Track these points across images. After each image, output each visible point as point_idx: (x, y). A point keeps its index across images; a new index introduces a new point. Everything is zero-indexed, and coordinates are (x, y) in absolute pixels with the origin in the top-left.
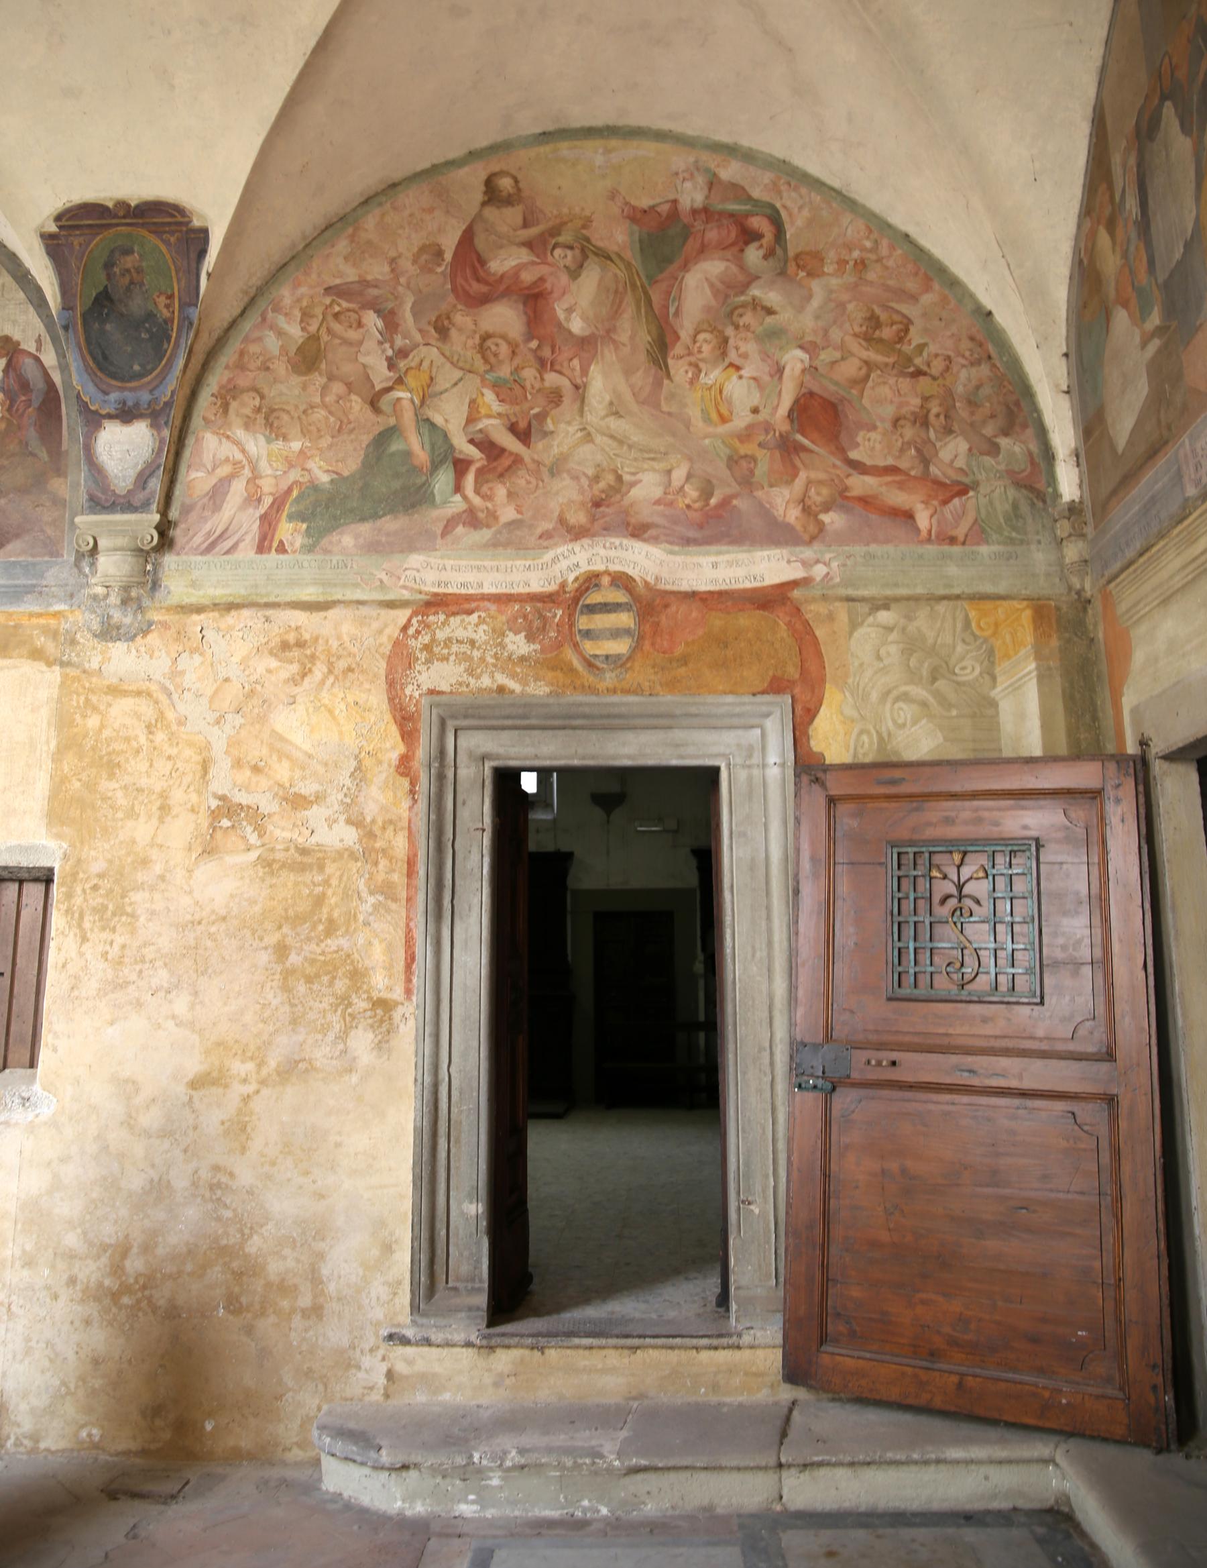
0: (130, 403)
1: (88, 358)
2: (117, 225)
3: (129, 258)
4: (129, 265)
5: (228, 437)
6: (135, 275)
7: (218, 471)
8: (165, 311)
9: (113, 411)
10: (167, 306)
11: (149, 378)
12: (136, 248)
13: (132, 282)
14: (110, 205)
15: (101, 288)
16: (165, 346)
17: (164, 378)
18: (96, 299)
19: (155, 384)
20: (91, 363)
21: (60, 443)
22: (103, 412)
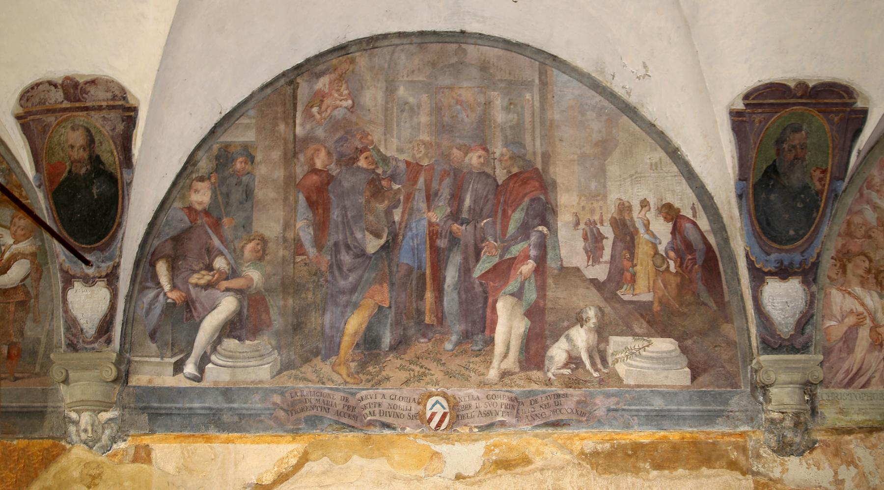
0: (786, 263)
1: (756, 223)
2: (794, 104)
3: (797, 136)
4: (796, 142)
5: (849, 293)
6: (799, 151)
7: (846, 320)
8: (818, 184)
9: (773, 269)
10: (820, 180)
11: (801, 241)
12: (804, 127)
13: (796, 158)
14: (792, 85)
15: (771, 163)
16: (815, 215)
17: (812, 243)
18: (766, 172)
19: (805, 246)
20: (757, 227)
21: (722, 295)
22: (766, 270)
